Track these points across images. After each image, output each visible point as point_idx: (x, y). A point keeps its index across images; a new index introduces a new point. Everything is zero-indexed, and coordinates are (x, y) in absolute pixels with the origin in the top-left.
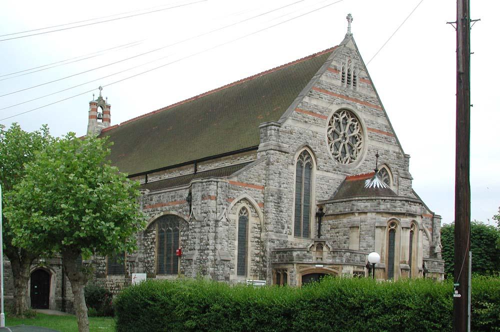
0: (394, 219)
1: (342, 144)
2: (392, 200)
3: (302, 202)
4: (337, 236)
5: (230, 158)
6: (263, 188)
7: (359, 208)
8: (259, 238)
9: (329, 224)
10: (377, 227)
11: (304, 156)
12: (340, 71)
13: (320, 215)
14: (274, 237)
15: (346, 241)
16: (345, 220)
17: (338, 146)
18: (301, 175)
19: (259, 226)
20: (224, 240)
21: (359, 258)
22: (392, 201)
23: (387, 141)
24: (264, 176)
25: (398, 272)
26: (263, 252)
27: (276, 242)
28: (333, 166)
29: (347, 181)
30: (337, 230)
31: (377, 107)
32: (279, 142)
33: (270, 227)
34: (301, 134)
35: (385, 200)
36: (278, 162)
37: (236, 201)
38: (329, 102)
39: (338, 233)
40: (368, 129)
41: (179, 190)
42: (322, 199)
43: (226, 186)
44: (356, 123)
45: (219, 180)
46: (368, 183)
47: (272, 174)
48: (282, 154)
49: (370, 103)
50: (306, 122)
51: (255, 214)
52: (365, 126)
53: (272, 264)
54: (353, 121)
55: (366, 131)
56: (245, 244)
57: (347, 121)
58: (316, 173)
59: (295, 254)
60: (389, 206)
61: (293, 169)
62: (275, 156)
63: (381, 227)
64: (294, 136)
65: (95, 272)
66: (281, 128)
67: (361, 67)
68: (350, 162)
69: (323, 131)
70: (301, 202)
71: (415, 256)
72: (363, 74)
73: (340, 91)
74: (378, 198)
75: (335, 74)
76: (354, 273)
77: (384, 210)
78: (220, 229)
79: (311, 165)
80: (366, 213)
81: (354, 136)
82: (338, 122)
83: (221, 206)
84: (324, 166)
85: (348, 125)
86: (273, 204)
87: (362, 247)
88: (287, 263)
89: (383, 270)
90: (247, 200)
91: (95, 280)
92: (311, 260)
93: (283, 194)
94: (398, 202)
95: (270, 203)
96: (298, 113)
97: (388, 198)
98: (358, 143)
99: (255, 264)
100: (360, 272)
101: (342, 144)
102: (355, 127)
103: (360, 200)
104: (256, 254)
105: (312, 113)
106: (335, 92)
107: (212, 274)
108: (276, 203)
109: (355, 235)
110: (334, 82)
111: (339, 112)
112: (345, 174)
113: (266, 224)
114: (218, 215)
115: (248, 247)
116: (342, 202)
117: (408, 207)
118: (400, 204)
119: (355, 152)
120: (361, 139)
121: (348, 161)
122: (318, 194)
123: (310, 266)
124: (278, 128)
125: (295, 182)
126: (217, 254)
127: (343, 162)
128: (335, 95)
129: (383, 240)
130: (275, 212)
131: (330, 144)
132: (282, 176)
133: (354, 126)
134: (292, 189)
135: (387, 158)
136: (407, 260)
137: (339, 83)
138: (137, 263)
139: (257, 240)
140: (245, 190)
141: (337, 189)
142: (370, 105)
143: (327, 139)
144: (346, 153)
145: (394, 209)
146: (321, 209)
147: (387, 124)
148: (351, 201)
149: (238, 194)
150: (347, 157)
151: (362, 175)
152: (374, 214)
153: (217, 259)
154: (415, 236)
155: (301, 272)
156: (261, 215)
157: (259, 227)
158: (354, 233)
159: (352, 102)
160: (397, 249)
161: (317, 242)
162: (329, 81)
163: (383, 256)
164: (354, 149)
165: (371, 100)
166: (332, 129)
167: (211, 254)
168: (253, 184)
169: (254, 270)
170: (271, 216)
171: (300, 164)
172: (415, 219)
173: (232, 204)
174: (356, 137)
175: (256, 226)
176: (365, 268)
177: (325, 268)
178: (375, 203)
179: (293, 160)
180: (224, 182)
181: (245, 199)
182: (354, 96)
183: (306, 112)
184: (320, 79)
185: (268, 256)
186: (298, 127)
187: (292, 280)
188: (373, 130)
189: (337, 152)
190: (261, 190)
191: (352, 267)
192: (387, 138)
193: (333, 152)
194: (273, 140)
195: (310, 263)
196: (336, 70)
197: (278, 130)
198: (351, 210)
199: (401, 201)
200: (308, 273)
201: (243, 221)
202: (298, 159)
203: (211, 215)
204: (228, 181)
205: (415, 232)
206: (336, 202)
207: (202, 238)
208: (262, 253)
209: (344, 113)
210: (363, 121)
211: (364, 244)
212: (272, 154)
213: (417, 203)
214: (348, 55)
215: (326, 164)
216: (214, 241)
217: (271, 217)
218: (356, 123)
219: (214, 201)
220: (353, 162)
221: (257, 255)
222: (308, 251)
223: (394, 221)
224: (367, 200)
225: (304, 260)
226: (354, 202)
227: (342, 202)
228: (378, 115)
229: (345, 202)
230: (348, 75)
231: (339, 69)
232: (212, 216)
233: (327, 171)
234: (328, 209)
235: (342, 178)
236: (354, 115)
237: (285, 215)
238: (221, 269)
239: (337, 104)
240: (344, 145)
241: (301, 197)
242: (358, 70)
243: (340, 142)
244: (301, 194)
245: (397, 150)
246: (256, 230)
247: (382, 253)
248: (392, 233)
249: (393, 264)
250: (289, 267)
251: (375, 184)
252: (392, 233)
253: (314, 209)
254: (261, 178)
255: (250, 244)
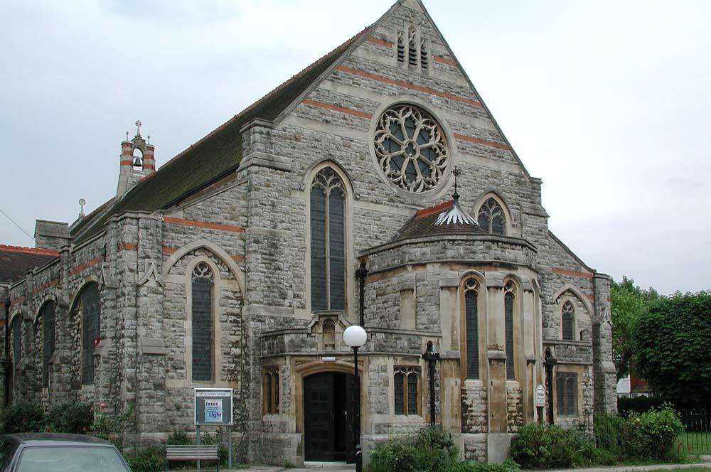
0: (472, 273)
1: (407, 161)
2: (466, 241)
3: (328, 253)
4: (386, 308)
5: (212, 189)
6: (243, 229)
7: (413, 258)
8: (239, 315)
9: (374, 289)
10: (442, 288)
11: (328, 179)
12: (392, 43)
13: (361, 275)
14: (263, 313)
15: (397, 315)
16: (394, 280)
17: (399, 164)
18: (324, 209)
19: (238, 295)
20: (152, 319)
21: (406, 343)
22: (468, 243)
23: (495, 156)
24: (244, 210)
25: (485, 365)
26: (245, 339)
27: (267, 322)
28: (388, 195)
29: (417, 218)
30: (384, 298)
31: (471, 101)
32: (270, 152)
33: (254, 296)
34: (317, 141)
35: (454, 241)
36: (268, 186)
37: (183, 251)
38: (374, 92)
39: (386, 302)
40: (456, 136)
41: (96, 240)
42: (364, 248)
43: (158, 226)
44: (434, 127)
45: (140, 215)
46: (442, 218)
47: (256, 206)
48: (278, 174)
49: (457, 95)
50: (327, 122)
51: (227, 274)
52: (450, 131)
53: (260, 359)
54: (426, 123)
55: (452, 140)
56: (210, 325)
57: (416, 124)
58: (351, 205)
59: (287, 339)
60: (462, 251)
61: (305, 198)
62: (260, 177)
63: (448, 288)
64: (302, 143)
65: (32, 383)
66: (273, 131)
67: (434, 39)
68: (425, 189)
69: (366, 138)
70: (325, 253)
71: (520, 337)
72: (441, 50)
73: (395, 74)
74: (442, 237)
75: (384, 48)
76: (395, 370)
77: (452, 257)
78: (142, 300)
79: (342, 192)
80: (424, 265)
81: (430, 148)
82: (396, 124)
83: (147, 260)
84: (369, 194)
85: (417, 131)
86: (259, 256)
87: (422, 324)
88: (277, 357)
89: (456, 362)
90: (209, 251)
91: (31, 395)
92: (315, 349)
93: (282, 239)
94: (479, 243)
95: (253, 255)
96: (310, 107)
97: (459, 237)
98: (439, 159)
99: (231, 360)
100: (410, 368)
101: (407, 161)
102: (432, 133)
103: (413, 243)
104: (233, 343)
105: (338, 107)
106: (384, 76)
107: (132, 379)
108: (265, 254)
109: (407, 303)
110: (383, 60)
111: (397, 107)
112: (415, 207)
113: (248, 290)
114: (140, 276)
115: (214, 332)
116: (389, 249)
117: (499, 252)
118: (482, 247)
119: (434, 173)
120: (444, 153)
121: (421, 187)
122: (360, 240)
123: (314, 359)
124: (269, 130)
125: (309, 222)
126: (139, 344)
127: (412, 189)
128: (386, 80)
129: (454, 310)
130: (266, 270)
131: (383, 160)
132: (278, 209)
133: (430, 131)
134: (301, 232)
135: (498, 182)
136: (502, 341)
137: (393, 61)
138: (58, 365)
139: (233, 318)
140: (202, 234)
141: (399, 231)
142: (459, 99)
143: (372, 150)
144: (416, 175)
145: (471, 255)
146: (363, 265)
147: (493, 129)
148: (400, 246)
149: (187, 240)
150: (418, 181)
151: (431, 209)
152: (437, 266)
153: (139, 353)
154: (517, 302)
155: (298, 371)
156: (240, 276)
157: (237, 297)
158: (406, 301)
159: (420, 92)
160: (482, 326)
161: (324, 316)
162: (371, 57)
163: (455, 337)
164: (431, 168)
165: (459, 90)
166: (384, 136)
167: (129, 344)
168: (220, 223)
169: (229, 370)
170: (255, 276)
171: (317, 192)
172: (513, 272)
173: (173, 258)
174: (436, 149)
175: (231, 294)
176: (420, 360)
177: (340, 362)
178: (438, 247)
179: (302, 183)
180: (151, 219)
181: (203, 249)
182: (424, 83)
183: (326, 105)
184: (354, 54)
185: (251, 344)
186: (311, 129)
187: (284, 385)
188: (466, 138)
189: (398, 172)
190: (238, 234)
191: (392, 359)
192: (494, 152)
193: (388, 172)
194: (258, 150)
195: (314, 353)
196: (384, 41)
197: (268, 133)
198: (402, 262)
199: (484, 241)
200: (312, 373)
201: (203, 288)
202: (314, 181)
203: (126, 276)
204: (160, 217)
205: (517, 295)
206: (382, 251)
207: (118, 318)
208: (244, 341)
209: (408, 110)
210: (445, 124)
211: (424, 319)
212: (256, 173)
213: (516, 245)
214: (408, 19)
215: (373, 190)
216: (134, 322)
217: (256, 278)
218: (434, 127)
219: (131, 253)
220: (430, 189)
221: (235, 344)
222: (308, 334)
223: (473, 276)
224: (425, 242)
225: (303, 350)
226: (404, 249)
227: (389, 249)
228: (475, 115)
229: (393, 248)
230: (422, 53)
231: (391, 40)
232: (129, 278)
233: (376, 203)
234: (372, 264)
235: (408, 214)
236: (429, 114)
237: (286, 275)
238: (144, 370)
239: (390, 95)
240: (411, 162)
241: (324, 244)
242: (430, 43)
243: (402, 156)
244: (324, 240)
245: (516, 170)
246: (230, 301)
247: (452, 332)
248: (471, 297)
249: (477, 352)
250: (280, 362)
251: (450, 217)
252: (471, 297)
253: (352, 265)
254: (236, 213)
255: (218, 326)
